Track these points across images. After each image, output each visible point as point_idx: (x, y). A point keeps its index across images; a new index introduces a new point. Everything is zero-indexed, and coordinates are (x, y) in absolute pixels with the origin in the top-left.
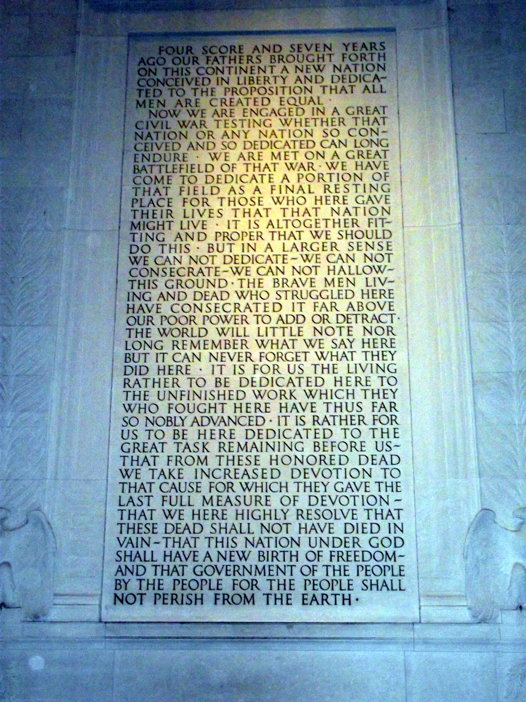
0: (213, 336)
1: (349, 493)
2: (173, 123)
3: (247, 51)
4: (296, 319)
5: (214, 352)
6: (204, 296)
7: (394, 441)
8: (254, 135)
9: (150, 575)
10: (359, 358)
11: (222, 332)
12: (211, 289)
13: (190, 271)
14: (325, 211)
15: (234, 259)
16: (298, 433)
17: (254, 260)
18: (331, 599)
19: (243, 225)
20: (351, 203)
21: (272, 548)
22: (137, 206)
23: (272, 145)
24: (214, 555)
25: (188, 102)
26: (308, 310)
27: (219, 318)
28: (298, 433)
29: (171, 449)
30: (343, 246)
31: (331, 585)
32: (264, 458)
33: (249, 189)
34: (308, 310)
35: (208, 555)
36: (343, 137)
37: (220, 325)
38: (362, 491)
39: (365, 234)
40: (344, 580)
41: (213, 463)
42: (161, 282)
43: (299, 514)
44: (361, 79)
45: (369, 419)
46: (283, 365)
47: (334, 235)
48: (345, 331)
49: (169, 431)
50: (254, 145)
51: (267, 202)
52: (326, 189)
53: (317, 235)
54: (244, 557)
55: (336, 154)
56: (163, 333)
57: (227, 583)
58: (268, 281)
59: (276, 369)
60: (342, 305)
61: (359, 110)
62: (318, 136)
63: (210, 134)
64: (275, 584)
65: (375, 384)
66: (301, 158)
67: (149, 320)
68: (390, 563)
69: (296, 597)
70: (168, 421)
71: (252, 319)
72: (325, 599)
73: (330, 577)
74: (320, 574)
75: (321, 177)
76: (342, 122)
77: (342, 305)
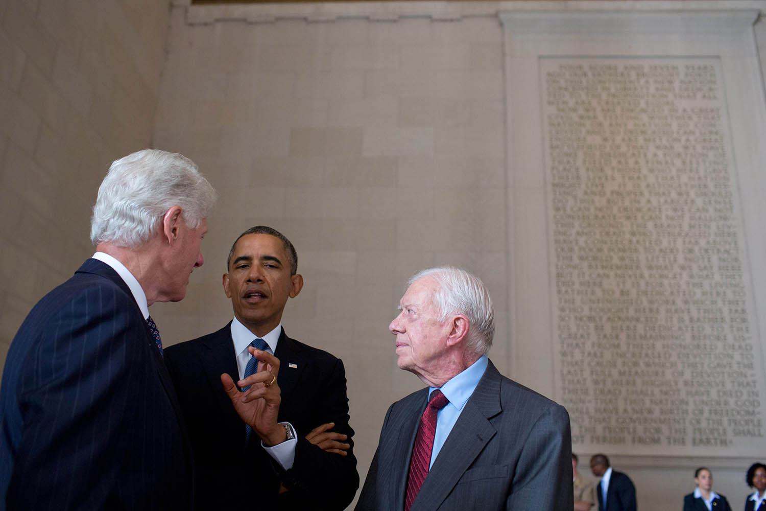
0: (616, 261)
1: (719, 370)
2: (575, 117)
3: (620, 69)
4: (672, 251)
5: (619, 272)
6: (607, 234)
7: (746, 335)
8: (630, 126)
9: (586, 423)
10: (717, 278)
11: (622, 259)
12: (612, 230)
13: (596, 217)
14: (684, 178)
15: (626, 209)
16: (680, 329)
17: (639, 210)
18: (713, 441)
19: (630, 186)
20: (702, 174)
21: (669, 406)
22: (555, 172)
23: (643, 132)
24: (630, 410)
25: (583, 102)
26: (679, 244)
27: (619, 249)
28: (680, 329)
29: (594, 338)
30: (699, 202)
31: (712, 431)
32: (659, 345)
33: (631, 162)
34: (679, 244)
35: (625, 411)
36: (692, 127)
37: (621, 254)
38: (727, 369)
39: (713, 194)
40: (721, 429)
41: (624, 348)
42: (577, 223)
43: (686, 383)
44: (700, 90)
45: (728, 319)
46: (666, 282)
47: (692, 194)
48: (706, 260)
49: (592, 325)
50: (631, 132)
51: (645, 171)
52: (684, 163)
53: (680, 194)
54: (650, 411)
55: (688, 140)
56: (582, 258)
57: (640, 429)
58: (650, 225)
59: (661, 285)
60: (703, 242)
61: (701, 110)
62: (675, 127)
63: (600, 124)
64: (673, 431)
65: (730, 296)
66: (664, 142)
67: (571, 250)
68: (751, 417)
69: (689, 440)
70: (591, 319)
71: (641, 249)
72: (708, 441)
73: (711, 427)
74: (704, 424)
75: (679, 155)
76: (690, 118)
77: (703, 242)
